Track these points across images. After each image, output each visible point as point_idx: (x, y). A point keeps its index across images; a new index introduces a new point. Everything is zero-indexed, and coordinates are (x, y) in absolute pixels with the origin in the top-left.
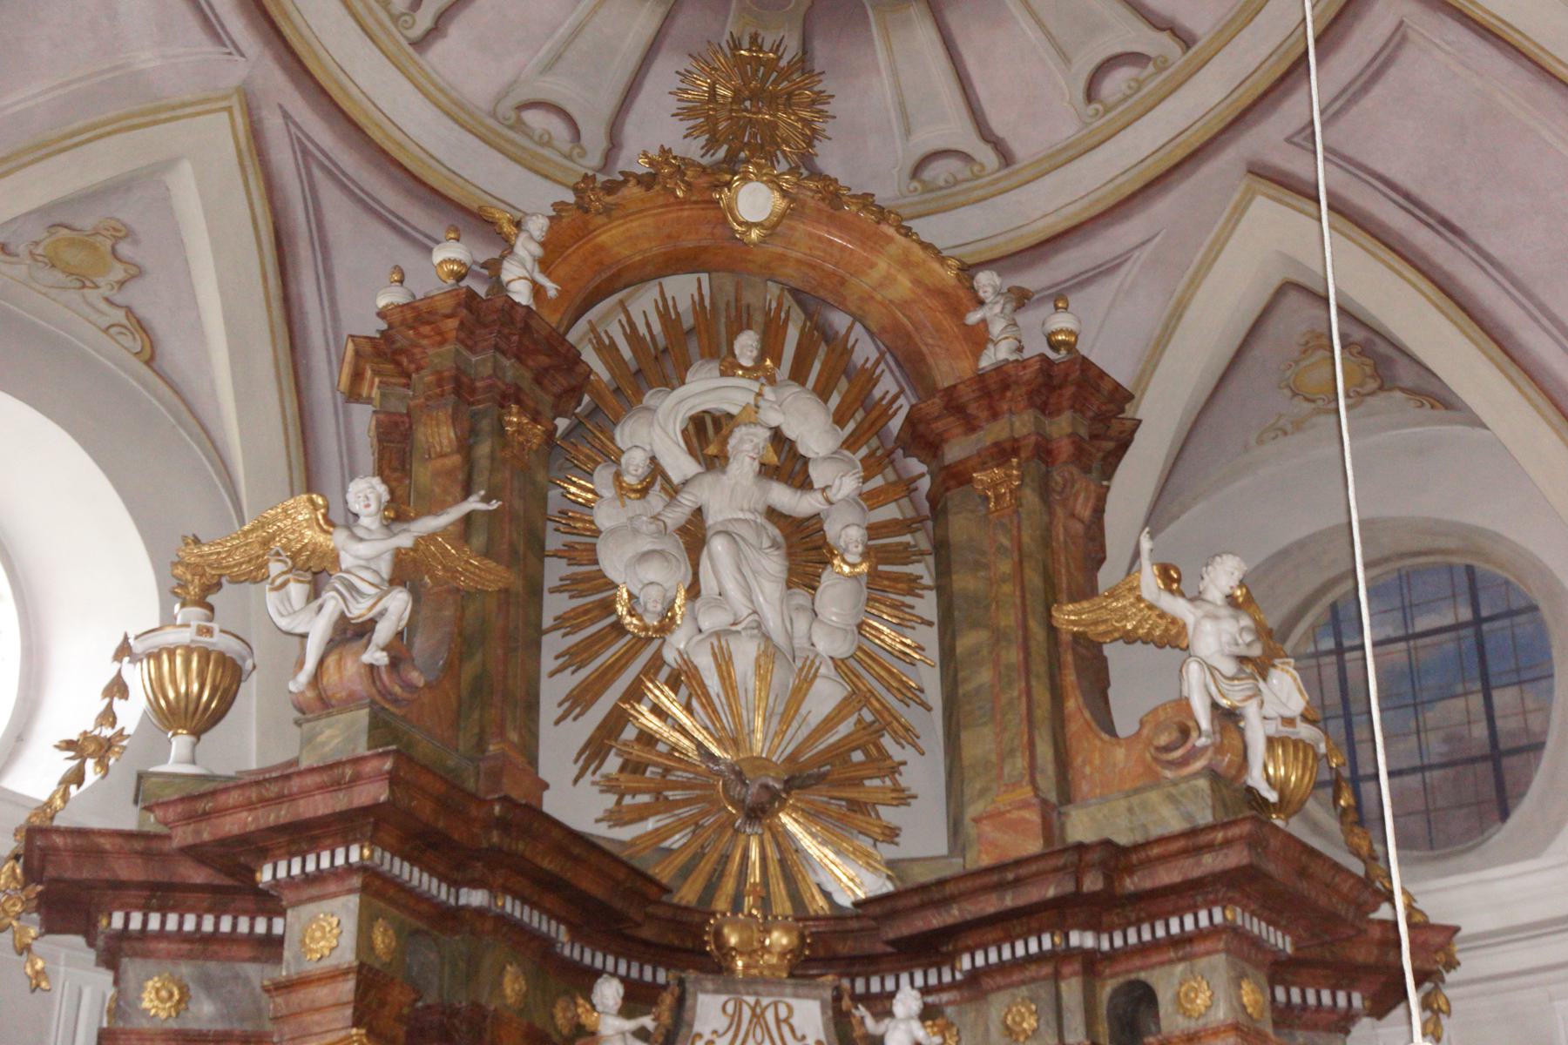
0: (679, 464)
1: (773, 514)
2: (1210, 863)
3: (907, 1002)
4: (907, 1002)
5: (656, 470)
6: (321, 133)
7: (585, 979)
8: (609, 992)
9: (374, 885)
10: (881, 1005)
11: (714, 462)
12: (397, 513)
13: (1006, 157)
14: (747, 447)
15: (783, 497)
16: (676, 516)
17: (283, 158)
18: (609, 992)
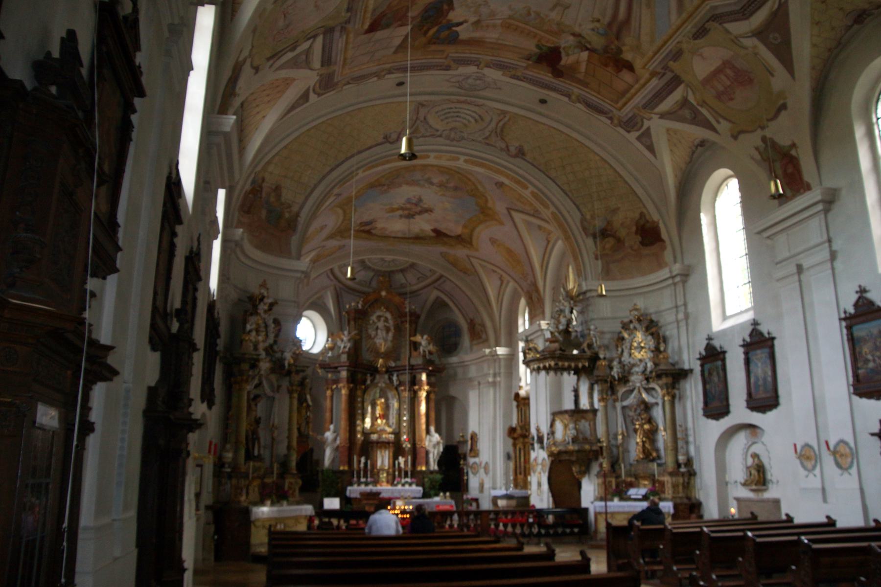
0: (376, 321)
1: (385, 326)
2: (419, 367)
3: (395, 375)
4: (395, 375)
5: (374, 322)
6: (341, 286)
7: (365, 374)
8: (369, 375)
9: (348, 370)
10: (393, 375)
11: (379, 320)
12: (349, 333)
13: (410, 284)
14: (382, 319)
15: (386, 324)
16: (375, 327)
17: (338, 289)
18: (369, 375)
